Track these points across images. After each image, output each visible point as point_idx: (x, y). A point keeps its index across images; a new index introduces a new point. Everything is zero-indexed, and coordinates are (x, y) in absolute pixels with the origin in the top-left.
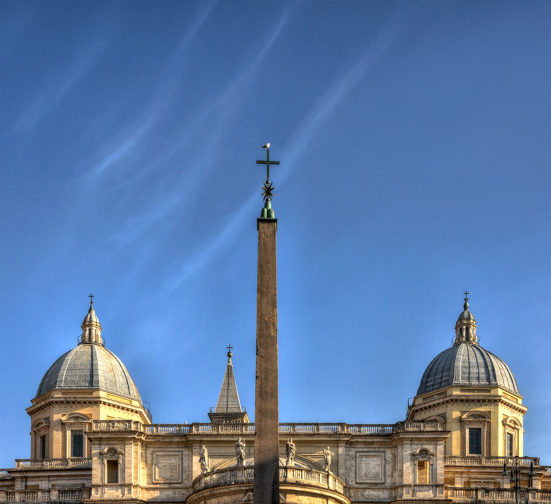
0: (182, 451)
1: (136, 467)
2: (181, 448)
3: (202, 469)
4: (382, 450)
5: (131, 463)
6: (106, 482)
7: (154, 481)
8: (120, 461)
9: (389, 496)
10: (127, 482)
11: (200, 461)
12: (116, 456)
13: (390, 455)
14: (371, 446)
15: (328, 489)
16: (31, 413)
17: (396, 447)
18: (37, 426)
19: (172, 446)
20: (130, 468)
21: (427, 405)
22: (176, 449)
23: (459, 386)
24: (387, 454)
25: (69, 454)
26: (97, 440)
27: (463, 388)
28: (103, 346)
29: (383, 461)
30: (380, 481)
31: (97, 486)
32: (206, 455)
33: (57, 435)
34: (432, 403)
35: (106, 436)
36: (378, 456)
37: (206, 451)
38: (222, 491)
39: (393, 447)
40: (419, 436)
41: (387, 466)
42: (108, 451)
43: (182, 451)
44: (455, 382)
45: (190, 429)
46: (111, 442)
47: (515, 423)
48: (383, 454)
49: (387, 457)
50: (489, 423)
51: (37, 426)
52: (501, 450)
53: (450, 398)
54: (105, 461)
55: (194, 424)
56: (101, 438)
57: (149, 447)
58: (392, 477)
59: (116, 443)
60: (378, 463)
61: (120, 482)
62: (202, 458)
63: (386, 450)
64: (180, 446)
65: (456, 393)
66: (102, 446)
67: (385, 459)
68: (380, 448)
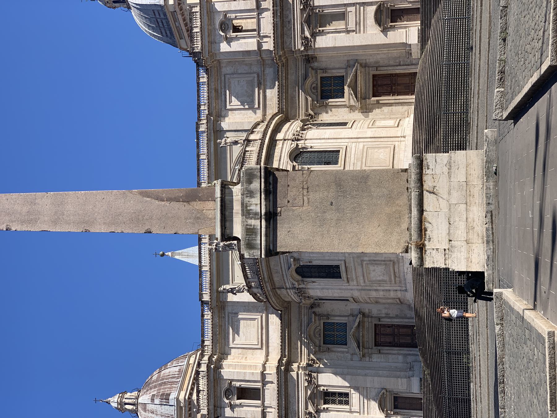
0: (229, 313)
1: (245, 367)
2: (225, 315)
3: (243, 292)
4: (223, 78)
5: (240, 373)
7: (259, 346)
8: (238, 384)
9: (271, 67)
10: (259, 378)
11: (235, 294)
12: (232, 389)
13: (228, 69)
14: (219, 92)
15: (263, 139)
17: (219, 61)
19: (223, 325)
20: (245, 373)
21: (186, 34)
22: (227, 320)
24: (228, 72)
26: (217, 410)
28: (140, 391)
29: (235, 76)
30: (256, 79)
32: (228, 287)
34: (184, 28)
35: (212, 400)
36: (230, 83)
37: (225, 287)
38: (264, 268)
39: (220, 65)
40: (207, 34)
41: (240, 72)
42: (227, 399)
43: (229, 313)
45: (206, 304)
46: (219, 395)
48: (227, 76)
49: (230, 72)
53: (177, 7)
55: (200, 300)
56: (215, 406)
57: (225, 351)
58: (251, 65)
59: (219, 388)
60: (236, 83)
61: (259, 385)
62: (232, 291)
63: (223, 73)
64: (223, 315)
66: (223, 406)
67: (233, 74)
68: (221, 80)
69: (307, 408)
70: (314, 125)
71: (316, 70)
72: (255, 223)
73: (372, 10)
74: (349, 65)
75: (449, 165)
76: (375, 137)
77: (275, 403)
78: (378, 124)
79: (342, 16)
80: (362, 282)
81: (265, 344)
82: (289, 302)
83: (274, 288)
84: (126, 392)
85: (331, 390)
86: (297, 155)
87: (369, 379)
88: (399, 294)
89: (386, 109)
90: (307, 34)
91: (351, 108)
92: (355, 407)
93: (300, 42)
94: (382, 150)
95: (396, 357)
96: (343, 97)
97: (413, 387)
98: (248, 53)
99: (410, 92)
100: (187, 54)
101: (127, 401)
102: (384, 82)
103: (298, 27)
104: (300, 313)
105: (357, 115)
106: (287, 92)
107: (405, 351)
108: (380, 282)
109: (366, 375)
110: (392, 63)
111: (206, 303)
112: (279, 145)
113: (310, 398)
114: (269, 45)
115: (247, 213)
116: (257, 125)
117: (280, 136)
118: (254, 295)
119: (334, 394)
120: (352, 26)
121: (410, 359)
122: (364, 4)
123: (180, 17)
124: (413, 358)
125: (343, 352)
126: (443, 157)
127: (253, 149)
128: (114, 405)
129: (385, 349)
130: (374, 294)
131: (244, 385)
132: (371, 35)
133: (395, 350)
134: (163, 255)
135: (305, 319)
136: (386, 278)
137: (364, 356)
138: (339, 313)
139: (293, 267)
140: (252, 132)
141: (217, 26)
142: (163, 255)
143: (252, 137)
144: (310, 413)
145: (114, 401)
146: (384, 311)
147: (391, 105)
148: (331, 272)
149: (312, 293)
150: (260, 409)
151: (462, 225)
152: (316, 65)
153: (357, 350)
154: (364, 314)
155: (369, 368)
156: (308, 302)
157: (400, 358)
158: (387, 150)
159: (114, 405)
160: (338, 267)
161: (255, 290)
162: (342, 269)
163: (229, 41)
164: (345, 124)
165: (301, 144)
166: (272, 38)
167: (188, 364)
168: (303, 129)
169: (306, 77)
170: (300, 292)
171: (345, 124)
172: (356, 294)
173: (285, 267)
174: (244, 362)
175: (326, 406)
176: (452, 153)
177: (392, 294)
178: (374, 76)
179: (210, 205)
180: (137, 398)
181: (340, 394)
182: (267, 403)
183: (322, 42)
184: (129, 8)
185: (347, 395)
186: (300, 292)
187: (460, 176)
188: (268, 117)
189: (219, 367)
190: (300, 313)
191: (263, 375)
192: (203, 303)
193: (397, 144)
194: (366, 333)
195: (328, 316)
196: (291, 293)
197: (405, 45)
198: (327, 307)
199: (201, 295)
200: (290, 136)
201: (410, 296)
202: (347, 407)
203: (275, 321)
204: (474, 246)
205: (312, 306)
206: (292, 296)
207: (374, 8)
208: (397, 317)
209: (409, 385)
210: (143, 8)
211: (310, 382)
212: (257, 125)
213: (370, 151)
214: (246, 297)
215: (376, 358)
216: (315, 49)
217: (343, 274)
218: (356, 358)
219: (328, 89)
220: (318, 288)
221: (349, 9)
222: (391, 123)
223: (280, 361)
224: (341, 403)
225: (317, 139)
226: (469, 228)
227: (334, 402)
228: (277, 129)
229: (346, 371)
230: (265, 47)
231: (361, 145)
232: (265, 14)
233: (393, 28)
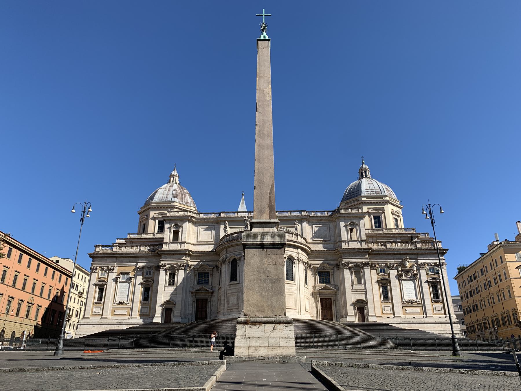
1: (189, 234)
6: (171, 241)
8: (180, 230)
16: (139, 214)
21: (348, 206)
23: (364, 197)
25: (156, 231)
27: (367, 197)
31: (166, 243)
32: (227, 225)
33: (151, 223)
34: (350, 205)
44: (362, 195)
47: (398, 213)
50: (384, 213)
52: (391, 224)
54: (172, 231)
61: (180, 241)
62: (225, 227)
65: (363, 199)
69: (168, 264)
70: (306, 268)
71: (333, 269)
72: (259, 238)
74: (336, 286)
75: (288, 338)
76: (301, 300)
77: (170, 248)
78: (307, 300)
79: (360, 283)
80: (229, 292)
81: (199, 244)
82: (219, 255)
83: (226, 248)
84: (179, 178)
85: (176, 276)
86: (291, 259)
87: (181, 296)
88: (222, 311)
89: (314, 305)
90: (350, 265)
91: (314, 287)
92: (167, 289)
93: (347, 261)
94: (294, 303)
95: (191, 310)
96: (320, 283)
97: (175, 319)
98: (340, 236)
99: (324, 317)
101: (175, 178)
102: (328, 304)
103: (354, 260)
104: (214, 261)
105: (311, 290)
106: (321, 254)
107: (194, 314)
108: (228, 302)
109: (182, 294)
110: (337, 308)
111: (220, 215)
112: (296, 251)
113: (172, 266)
114: (344, 246)
115: (264, 234)
116: (305, 240)
117: (300, 251)
118: (223, 238)
119: (174, 278)
120: (355, 288)
121: (190, 317)
122: (366, 294)
123: (356, 203)
124: (190, 319)
125: (194, 282)
126: (292, 334)
127: (294, 238)
128: (173, 173)
129: (195, 304)
130: (222, 298)
131: (180, 233)
132: (351, 298)
133: (194, 309)
134: (243, 195)
135: (211, 263)
136: (230, 305)
137: (192, 293)
138: (213, 280)
139: (236, 257)
140: (301, 237)
141: (352, 221)
142: (243, 195)
143: (299, 237)
144: (165, 266)
145: (175, 172)
146: (214, 304)
147: (317, 307)
148: (234, 276)
149: (224, 266)
150: (168, 241)
151: (257, 344)
152: (336, 269)
153: (195, 290)
154: (212, 293)
155: (186, 295)
156: (219, 265)
157: (191, 312)
158: (294, 306)
159: (173, 173)
160: (236, 280)
161: (225, 239)
162: (235, 282)
163: (346, 226)
164: (306, 284)
165: (296, 261)
166: (360, 247)
167: (191, 207)
168: (303, 262)
169: (329, 264)
170: (224, 261)
171: (306, 284)
172: (223, 289)
173: (237, 253)
174: (191, 233)
175: (168, 274)
176: (294, 339)
177: (222, 308)
178: (331, 299)
179: (268, 217)
180: (176, 183)
181: (174, 281)
182: (171, 244)
183: (347, 272)
184: (359, 179)
185: (173, 284)
186: (224, 261)
187: (282, 343)
188: (309, 245)
189: (189, 221)
190: (214, 261)
191: (184, 243)
192: (220, 213)
193: (297, 310)
194: (203, 294)
195: (212, 275)
196: (224, 256)
197: (347, 315)
198: (216, 274)
199: (223, 213)
200: (300, 256)
201: (221, 317)
202: (167, 285)
203: (210, 248)
204: (247, 350)
205: (217, 267)
206: (223, 257)
207: (364, 299)
208: (211, 310)
209: (177, 316)
210: (359, 186)
211: (180, 266)
212: (305, 240)
213: (293, 296)
214: (222, 234)
215: (191, 299)
216: (343, 269)
217: (232, 283)
218: (191, 289)
219: (324, 276)
220: (226, 270)
221: (363, 286)
222: (308, 308)
223: (191, 251)
224: (170, 281)
225: (299, 269)
226: (256, 348)
227: (170, 278)
228: (303, 250)
229: (185, 284)
230: (343, 244)
231: (296, 292)
232: (359, 244)
233: (355, 309)
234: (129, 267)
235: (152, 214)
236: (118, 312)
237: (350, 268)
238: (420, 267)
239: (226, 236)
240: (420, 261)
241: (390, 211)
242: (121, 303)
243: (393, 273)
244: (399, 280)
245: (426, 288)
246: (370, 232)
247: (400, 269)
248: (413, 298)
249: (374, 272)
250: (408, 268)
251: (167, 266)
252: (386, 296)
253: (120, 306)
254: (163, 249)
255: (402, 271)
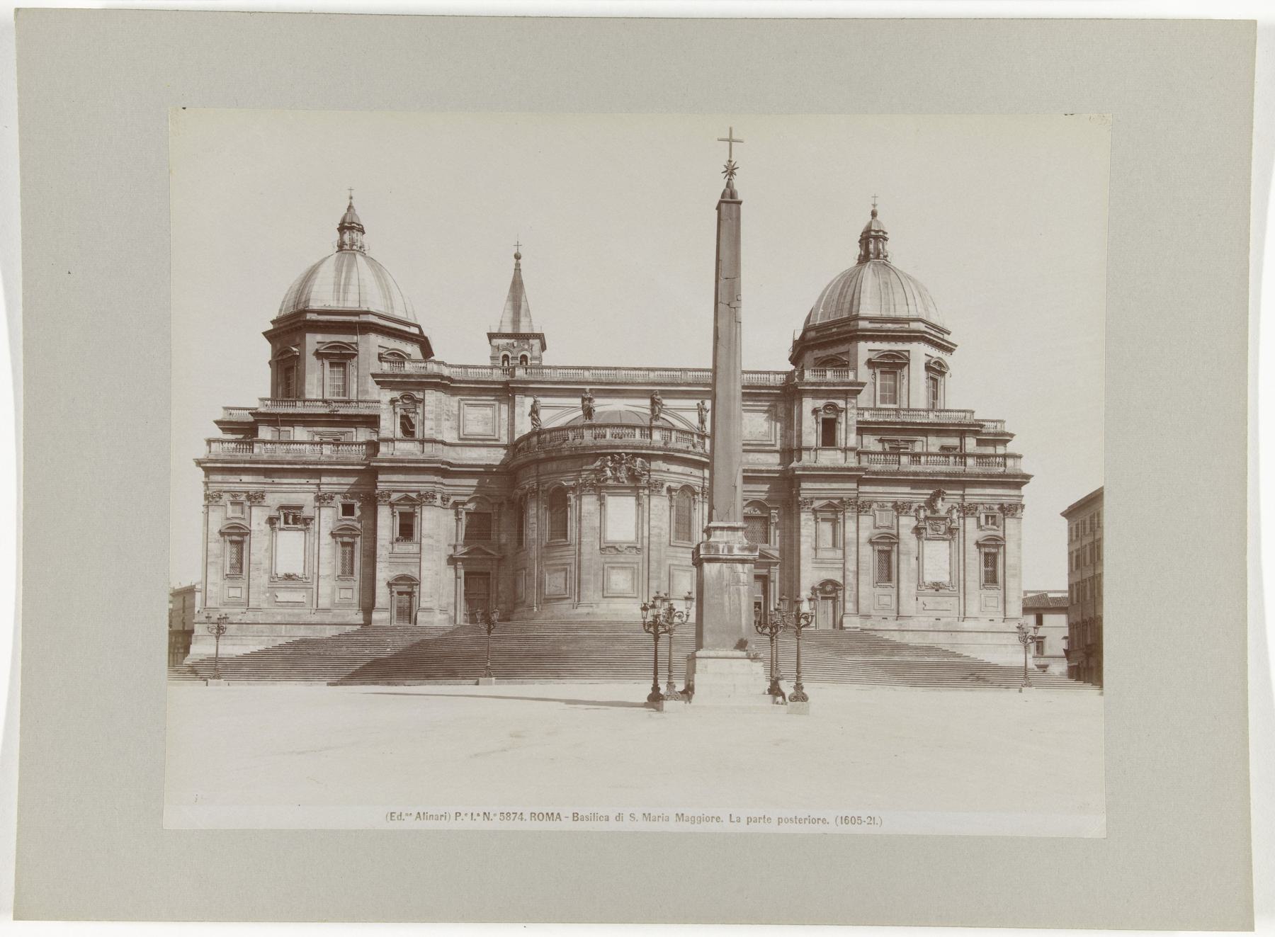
18: (282, 354)
51: (282, 354)
61: (418, 435)
73: (837, 577)
77: (398, 454)
79: (834, 545)
81: (467, 442)
85: (417, 521)
90: (817, 504)
93: (808, 496)
100: (797, 337)
120: (821, 554)
144: (389, 496)
148: (560, 528)
175: (397, 514)
206: (529, 483)
214: (524, 426)
221: (839, 553)
230: (805, 455)
234: (301, 494)
235: (313, 341)
236: (283, 596)
237: (815, 511)
238: (967, 510)
239: (538, 432)
240: (968, 500)
241: (924, 360)
242: (289, 577)
243: (907, 522)
244: (919, 539)
245: (974, 559)
246: (867, 416)
247: (922, 515)
248: (945, 578)
249: (866, 521)
250: (943, 513)
251: (395, 496)
252: (887, 572)
253: (291, 583)
254: (379, 456)
255: (927, 518)
